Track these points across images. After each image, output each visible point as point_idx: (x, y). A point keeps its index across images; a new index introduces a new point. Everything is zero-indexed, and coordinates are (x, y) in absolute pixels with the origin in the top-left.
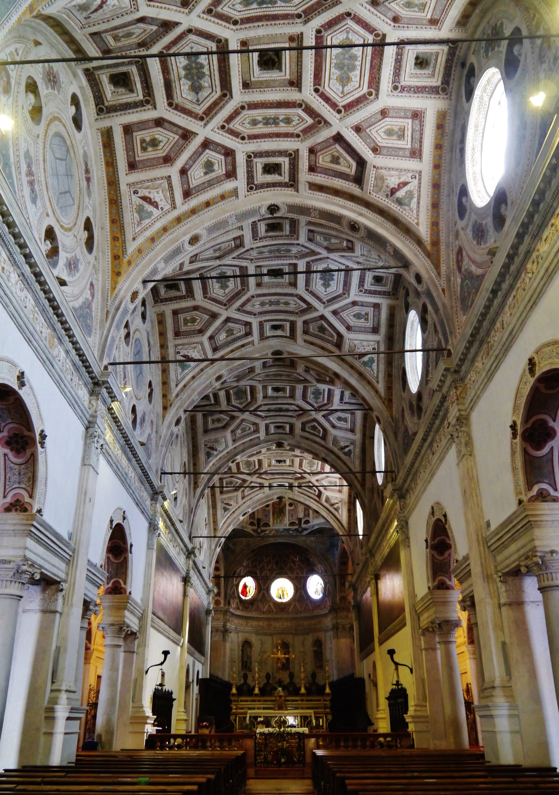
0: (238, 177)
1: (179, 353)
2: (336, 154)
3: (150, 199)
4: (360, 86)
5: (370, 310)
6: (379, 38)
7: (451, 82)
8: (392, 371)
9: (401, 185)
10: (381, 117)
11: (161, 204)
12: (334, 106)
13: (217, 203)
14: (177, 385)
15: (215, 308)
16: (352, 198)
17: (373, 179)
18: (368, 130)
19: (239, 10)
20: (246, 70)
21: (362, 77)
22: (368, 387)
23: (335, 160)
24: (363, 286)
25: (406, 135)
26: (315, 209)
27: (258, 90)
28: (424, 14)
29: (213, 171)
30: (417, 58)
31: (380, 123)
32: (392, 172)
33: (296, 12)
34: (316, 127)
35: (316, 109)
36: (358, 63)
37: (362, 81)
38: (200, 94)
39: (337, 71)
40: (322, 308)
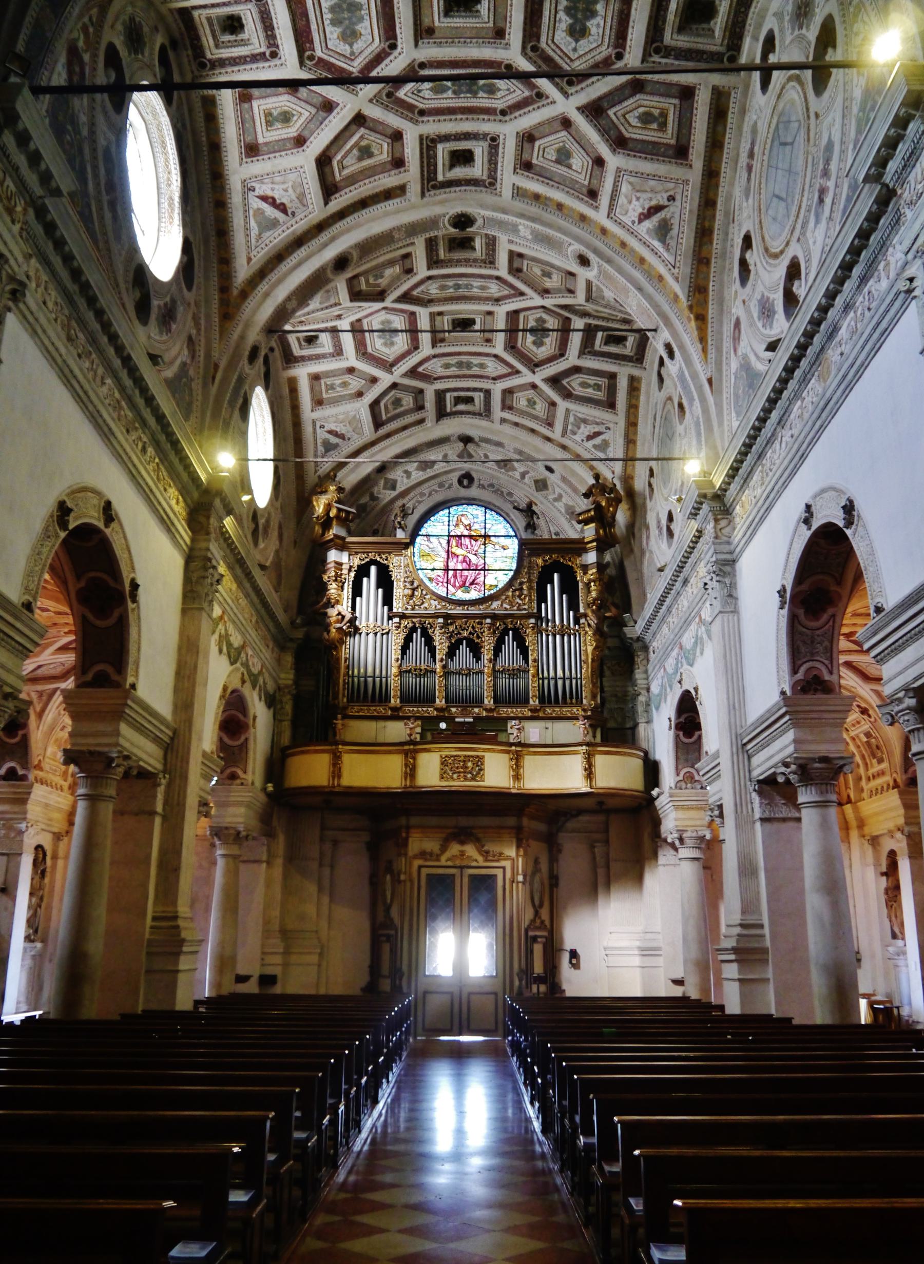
6: (308, 53)
23: (366, 152)
28: (262, 108)
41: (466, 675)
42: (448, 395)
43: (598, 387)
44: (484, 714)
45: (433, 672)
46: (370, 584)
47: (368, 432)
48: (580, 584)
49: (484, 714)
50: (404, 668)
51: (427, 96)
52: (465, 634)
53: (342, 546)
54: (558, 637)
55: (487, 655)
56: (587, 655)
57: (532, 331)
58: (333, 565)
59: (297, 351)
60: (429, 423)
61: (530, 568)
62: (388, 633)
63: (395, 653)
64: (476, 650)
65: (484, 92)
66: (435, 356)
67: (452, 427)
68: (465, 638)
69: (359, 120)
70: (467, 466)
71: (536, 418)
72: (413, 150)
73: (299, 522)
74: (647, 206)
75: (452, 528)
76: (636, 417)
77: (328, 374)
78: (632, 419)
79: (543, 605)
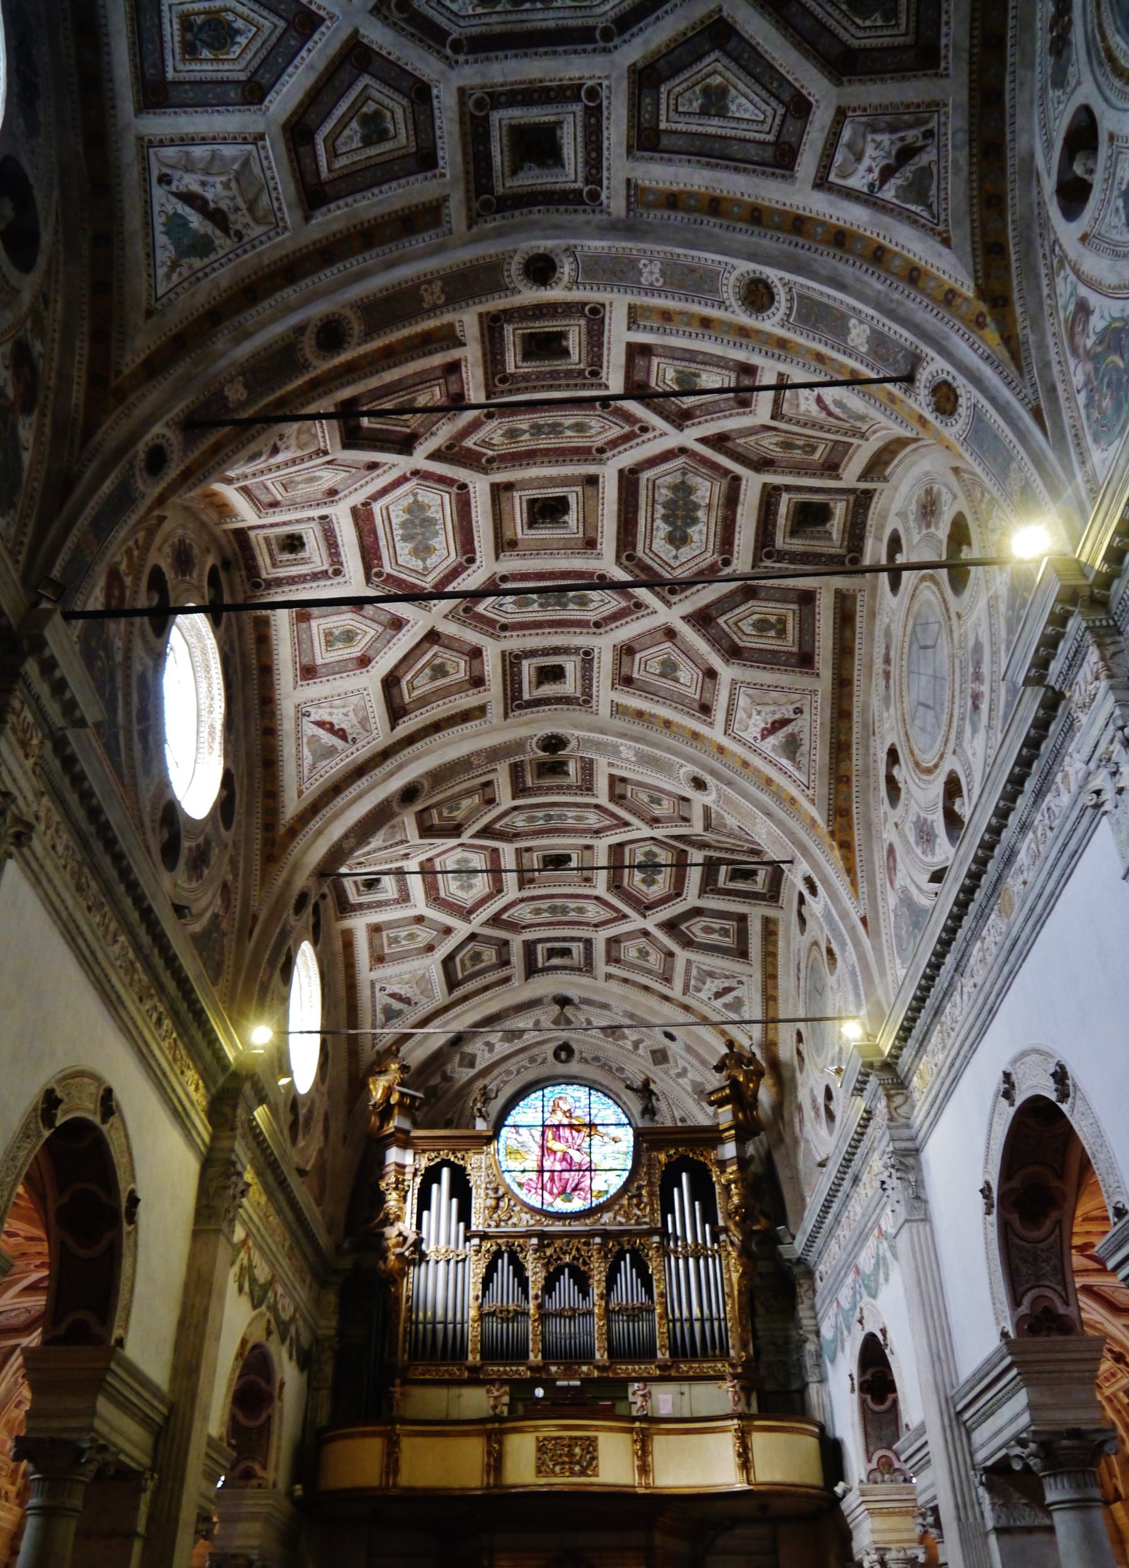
6: (375, 570)
23: (439, 671)
41: (570, 1318)
42: (539, 947)
43: (725, 932)
44: (596, 1374)
45: (526, 1314)
46: (441, 1192)
47: (440, 994)
48: (717, 1187)
49: (596, 1374)
50: (486, 1309)
52: (567, 1259)
53: (405, 1142)
54: (691, 1261)
55: (597, 1289)
56: (731, 1286)
57: (641, 867)
58: (393, 1167)
59: (353, 898)
60: (516, 982)
61: (650, 1166)
62: (464, 1260)
63: (474, 1288)
64: (582, 1282)
66: (522, 900)
67: (544, 986)
68: (567, 1265)
69: (432, 637)
70: (565, 1035)
71: (649, 972)
72: (494, 666)
73: (350, 1111)
74: (770, 721)
75: (547, 1115)
76: (775, 966)
77: (391, 925)
78: (770, 969)
79: (669, 1217)
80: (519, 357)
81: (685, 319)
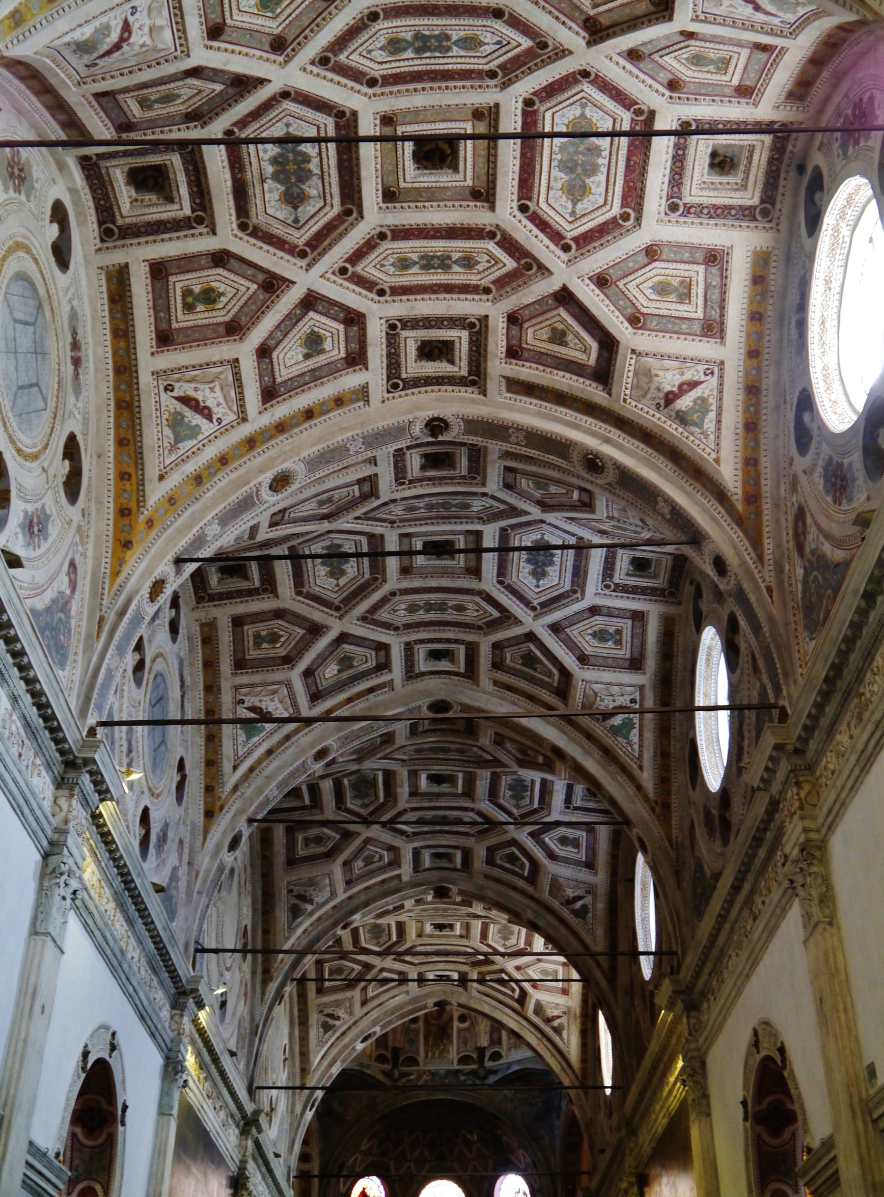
0: (371, 365)
1: (242, 702)
2: (560, 326)
3: (197, 401)
4: (605, 203)
5: (626, 625)
7: (779, 198)
8: (669, 745)
9: (685, 387)
10: (646, 261)
11: (218, 412)
12: (556, 236)
13: (329, 411)
14: (235, 768)
15: (317, 614)
16: (590, 409)
17: (631, 374)
18: (621, 284)
19: (379, 60)
20: (390, 168)
21: (611, 187)
22: (621, 778)
23: (559, 337)
24: (611, 576)
25: (693, 294)
26: (519, 429)
27: (413, 205)
28: (727, 78)
29: (322, 351)
30: (714, 155)
31: (644, 271)
32: (667, 363)
33: (486, 67)
34: (522, 275)
35: (522, 242)
36: (602, 161)
37: (610, 194)
38: (300, 209)
39: (563, 175)
40: (530, 619)
51: (489, 35)
57: (346, 556)
65: (405, 40)
80: (457, 346)
81: (325, 408)
